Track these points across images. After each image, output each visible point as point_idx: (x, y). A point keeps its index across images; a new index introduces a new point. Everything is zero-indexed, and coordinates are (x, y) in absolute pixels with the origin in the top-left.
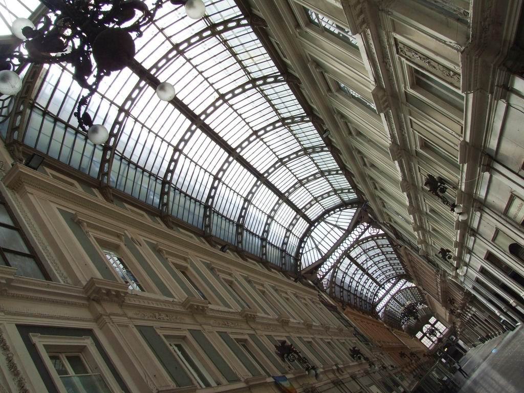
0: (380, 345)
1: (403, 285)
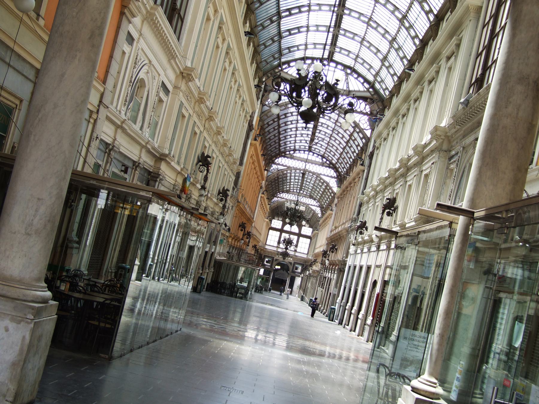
0: (239, 201)
1: (328, 176)
